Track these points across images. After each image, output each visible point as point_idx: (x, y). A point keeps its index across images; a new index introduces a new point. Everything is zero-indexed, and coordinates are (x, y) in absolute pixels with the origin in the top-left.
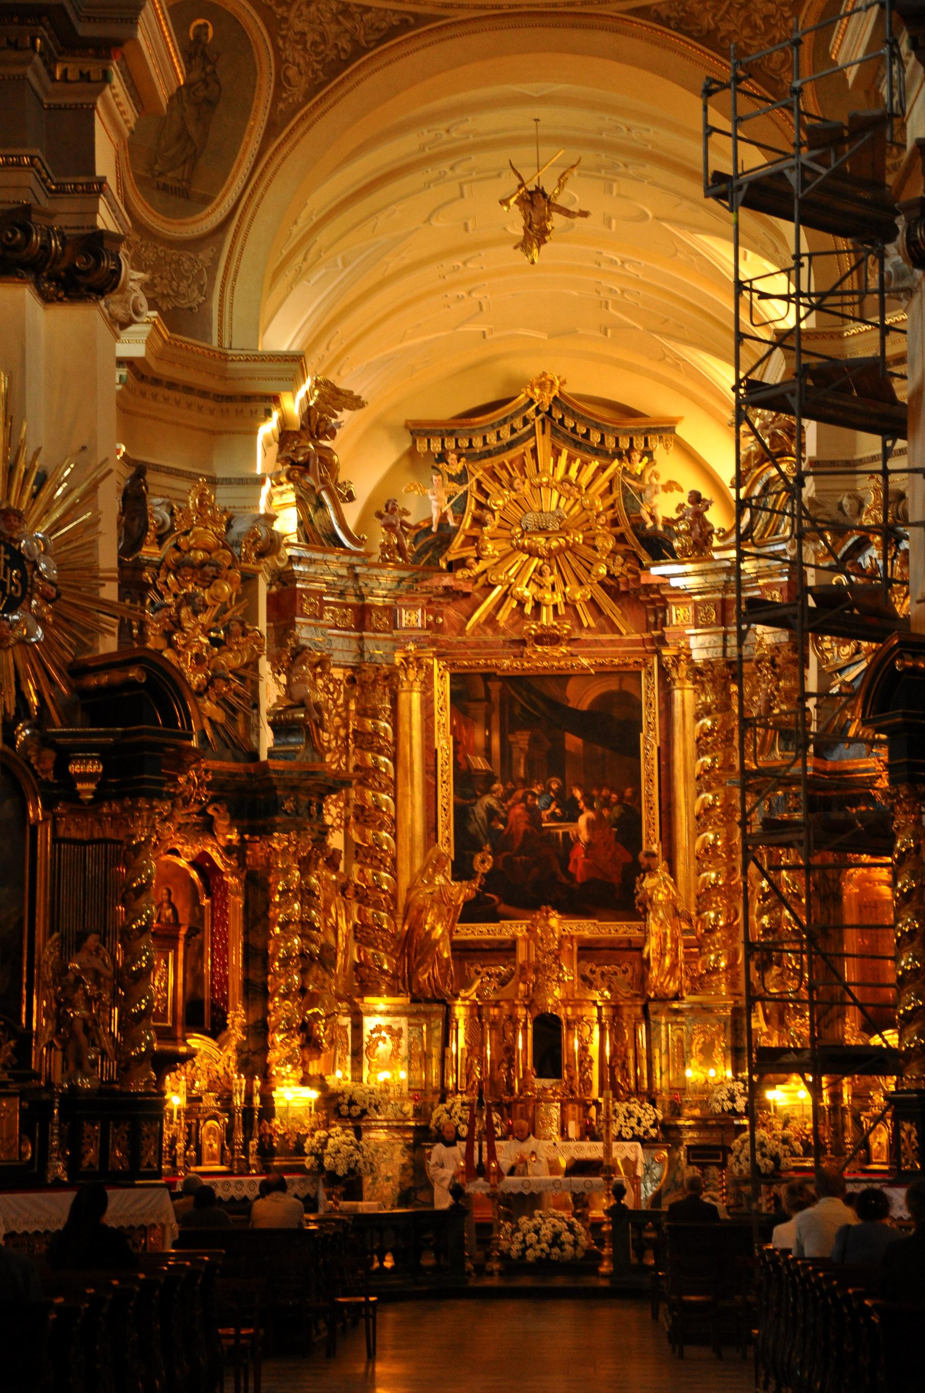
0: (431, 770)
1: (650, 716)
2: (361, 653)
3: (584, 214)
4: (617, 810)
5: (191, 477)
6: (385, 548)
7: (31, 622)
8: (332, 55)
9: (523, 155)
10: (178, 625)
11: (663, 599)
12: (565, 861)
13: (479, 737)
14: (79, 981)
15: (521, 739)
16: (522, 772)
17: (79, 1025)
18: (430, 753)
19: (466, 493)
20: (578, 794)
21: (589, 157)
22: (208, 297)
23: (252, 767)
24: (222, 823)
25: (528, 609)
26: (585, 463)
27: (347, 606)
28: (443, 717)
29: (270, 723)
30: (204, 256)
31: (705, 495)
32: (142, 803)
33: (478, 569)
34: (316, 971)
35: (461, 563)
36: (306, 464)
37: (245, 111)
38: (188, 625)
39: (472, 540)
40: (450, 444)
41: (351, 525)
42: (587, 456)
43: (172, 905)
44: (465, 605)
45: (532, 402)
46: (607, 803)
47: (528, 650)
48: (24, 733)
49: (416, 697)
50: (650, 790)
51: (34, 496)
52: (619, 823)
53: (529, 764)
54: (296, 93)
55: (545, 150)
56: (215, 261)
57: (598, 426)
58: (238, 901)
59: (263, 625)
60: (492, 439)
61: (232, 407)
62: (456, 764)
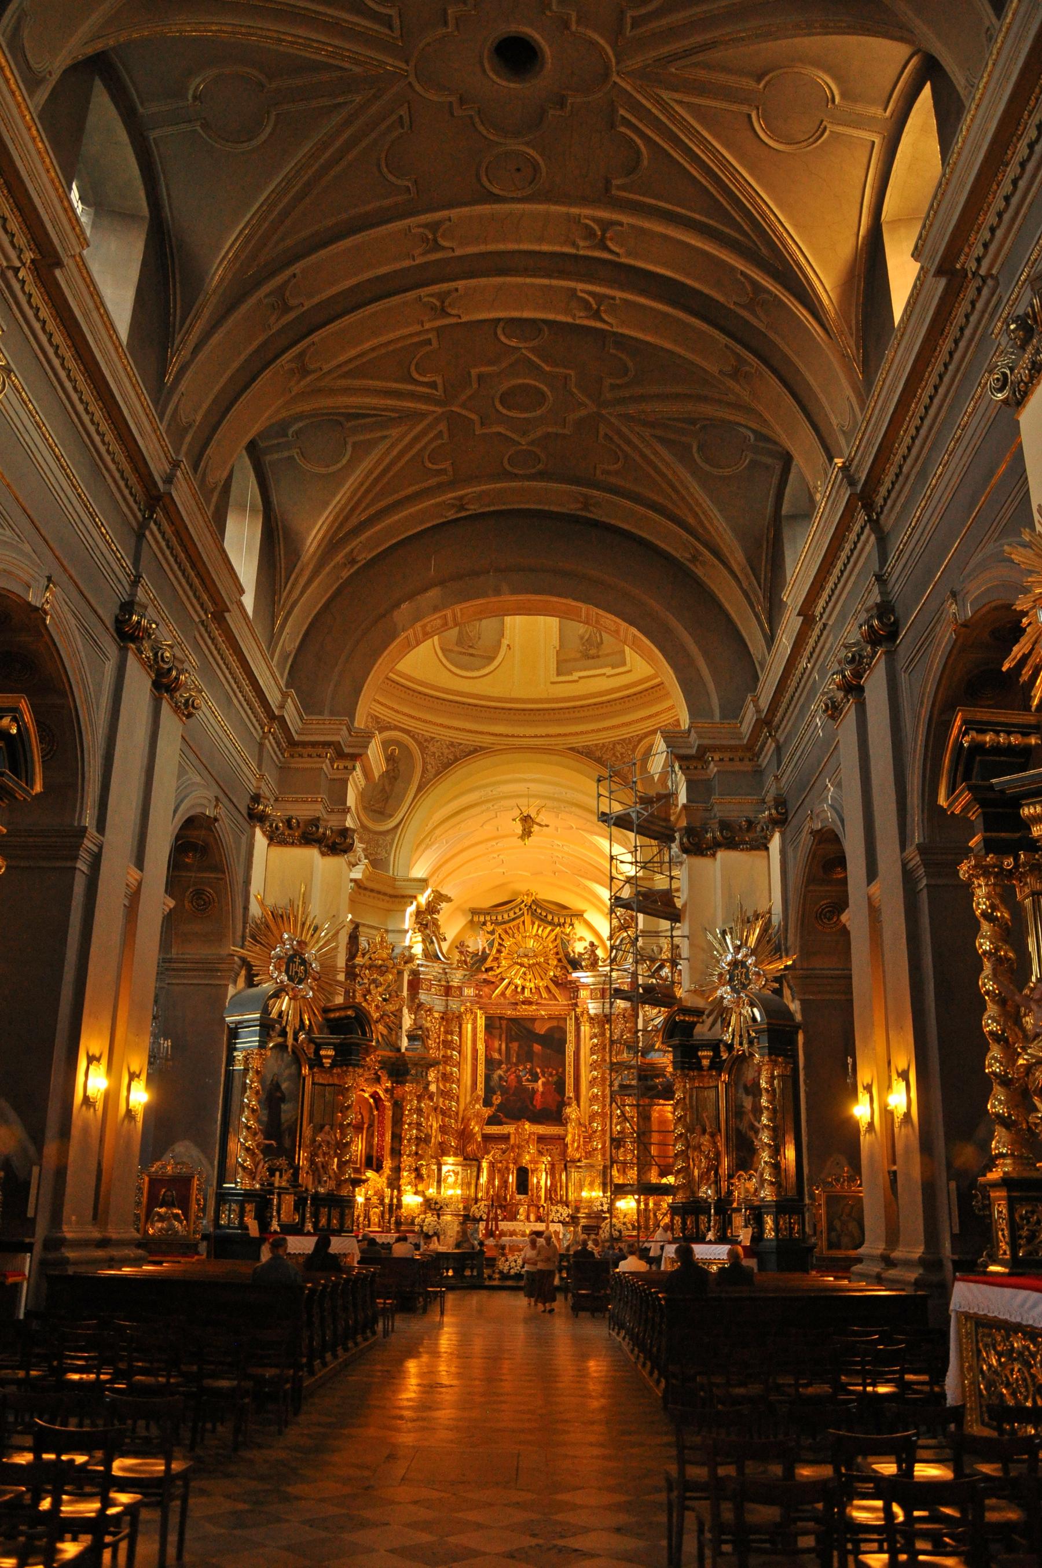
0: (475, 1058)
1: (571, 1037)
2: (447, 1006)
3: (547, 826)
4: (555, 1078)
5: (378, 929)
6: (459, 961)
7: (308, 989)
8: (446, 760)
9: (522, 801)
10: (369, 992)
12: (532, 1099)
13: (496, 1044)
14: (320, 1145)
15: (515, 1046)
16: (514, 1060)
17: (320, 1165)
18: (475, 1050)
20: (538, 1070)
21: (549, 803)
22: (389, 855)
23: (398, 1055)
24: (384, 1078)
25: (519, 990)
26: (545, 928)
28: (481, 1035)
29: (407, 1036)
30: (389, 838)
31: (596, 943)
32: (351, 1069)
33: (498, 971)
34: (423, 1145)
35: (491, 969)
36: (426, 925)
37: (409, 782)
38: (373, 992)
39: (496, 959)
41: (444, 951)
44: (492, 986)
46: (551, 1075)
48: (302, 1036)
49: (470, 1026)
50: (570, 1070)
51: (312, 935)
52: (555, 1083)
55: (532, 800)
56: (393, 840)
57: (551, 913)
58: (389, 1113)
59: (405, 993)
60: (506, 916)
61: (397, 900)
62: (486, 1056)
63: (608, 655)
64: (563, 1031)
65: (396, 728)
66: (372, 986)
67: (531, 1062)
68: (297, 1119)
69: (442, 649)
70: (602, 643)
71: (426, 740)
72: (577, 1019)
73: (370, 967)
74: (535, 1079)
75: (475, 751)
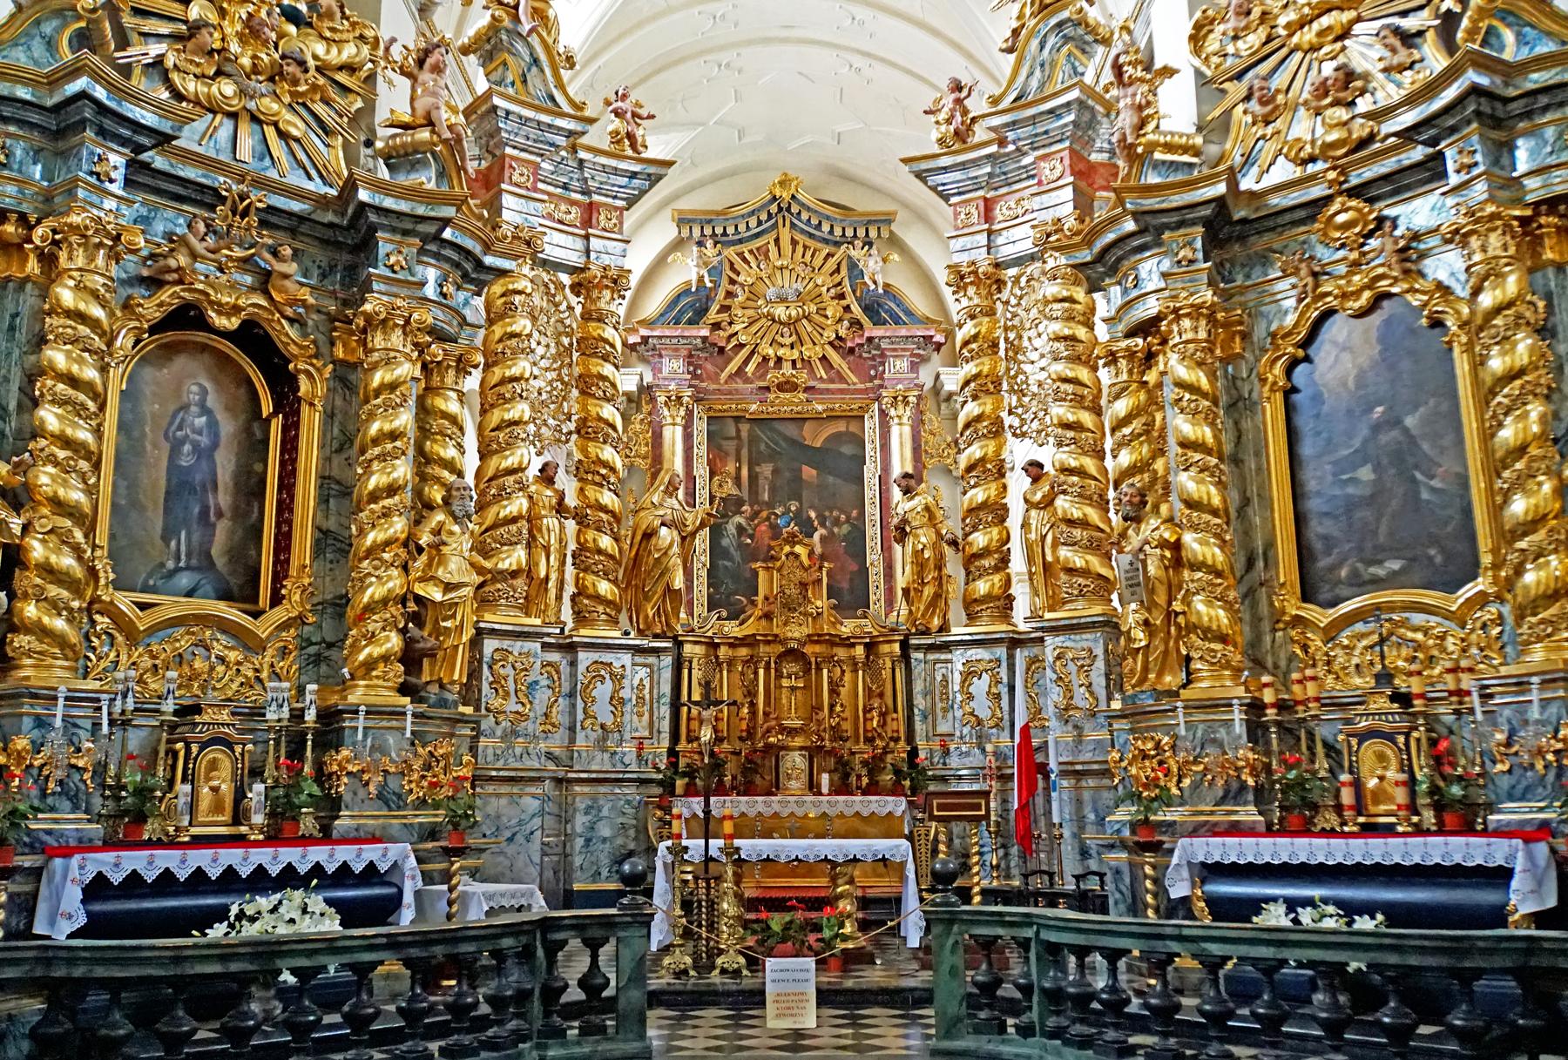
4: (845, 529)
11: (883, 355)
13: (731, 467)
15: (766, 470)
20: (813, 514)
25: (771, 364)
27: (573, 203)
31: (965, 80)
35: (716, 326)
39: (725, 309)
40: (708, 231)
42: (819, 245)
43: (205, 410)
44: (720, 360)
45: (774, 198)
46: (837, 522)
47: (771, 396)
49: (679, 431)
53: (773, 490)
60: (742, 227)
72: (883, 413)
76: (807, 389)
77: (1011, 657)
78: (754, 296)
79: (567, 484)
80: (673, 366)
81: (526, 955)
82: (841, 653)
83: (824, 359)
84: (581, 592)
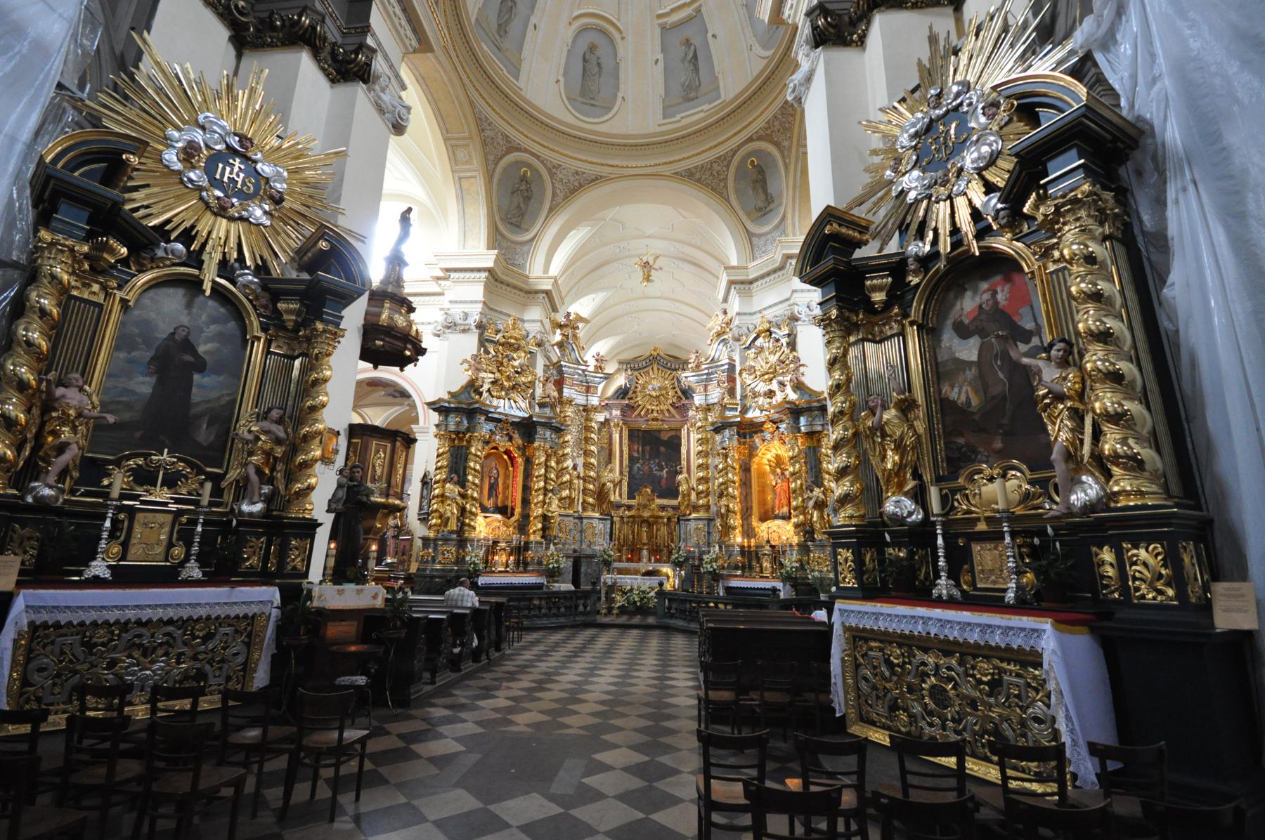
0: (621, 456)
1: (684, 442)
10: (502, 364)
12: (659, 482)
13: (636, 447)
15: (648, 448)
19: (632, 380)
22: (526, 262)
28: (625, 441)
30: (525, 248)
35: (631, 399)
37: (542, 203)
39: (634, 392)
49: (618, 435)
54: (559, 199)
56: (529, 250)
58: (521, 468)
61: (531, 296)
63: (706, 94)
64: (679, 438)
65: (526, 151)
66: (505, 360)
67: (658, 458)
68: (234, 401)
69: (568, 98)
70: (700, 85)
71: (554, 167)
73: (503, 345)
74: (661, 469)
75: (597, 179)
76: (662, 421)
77: (708, 524)
78: (644, 387)
79: (580, 469)
80: (616, 413)
81: (571, 598)
82: (660, 521)
83: (668, 410)
84: (584, 501)
